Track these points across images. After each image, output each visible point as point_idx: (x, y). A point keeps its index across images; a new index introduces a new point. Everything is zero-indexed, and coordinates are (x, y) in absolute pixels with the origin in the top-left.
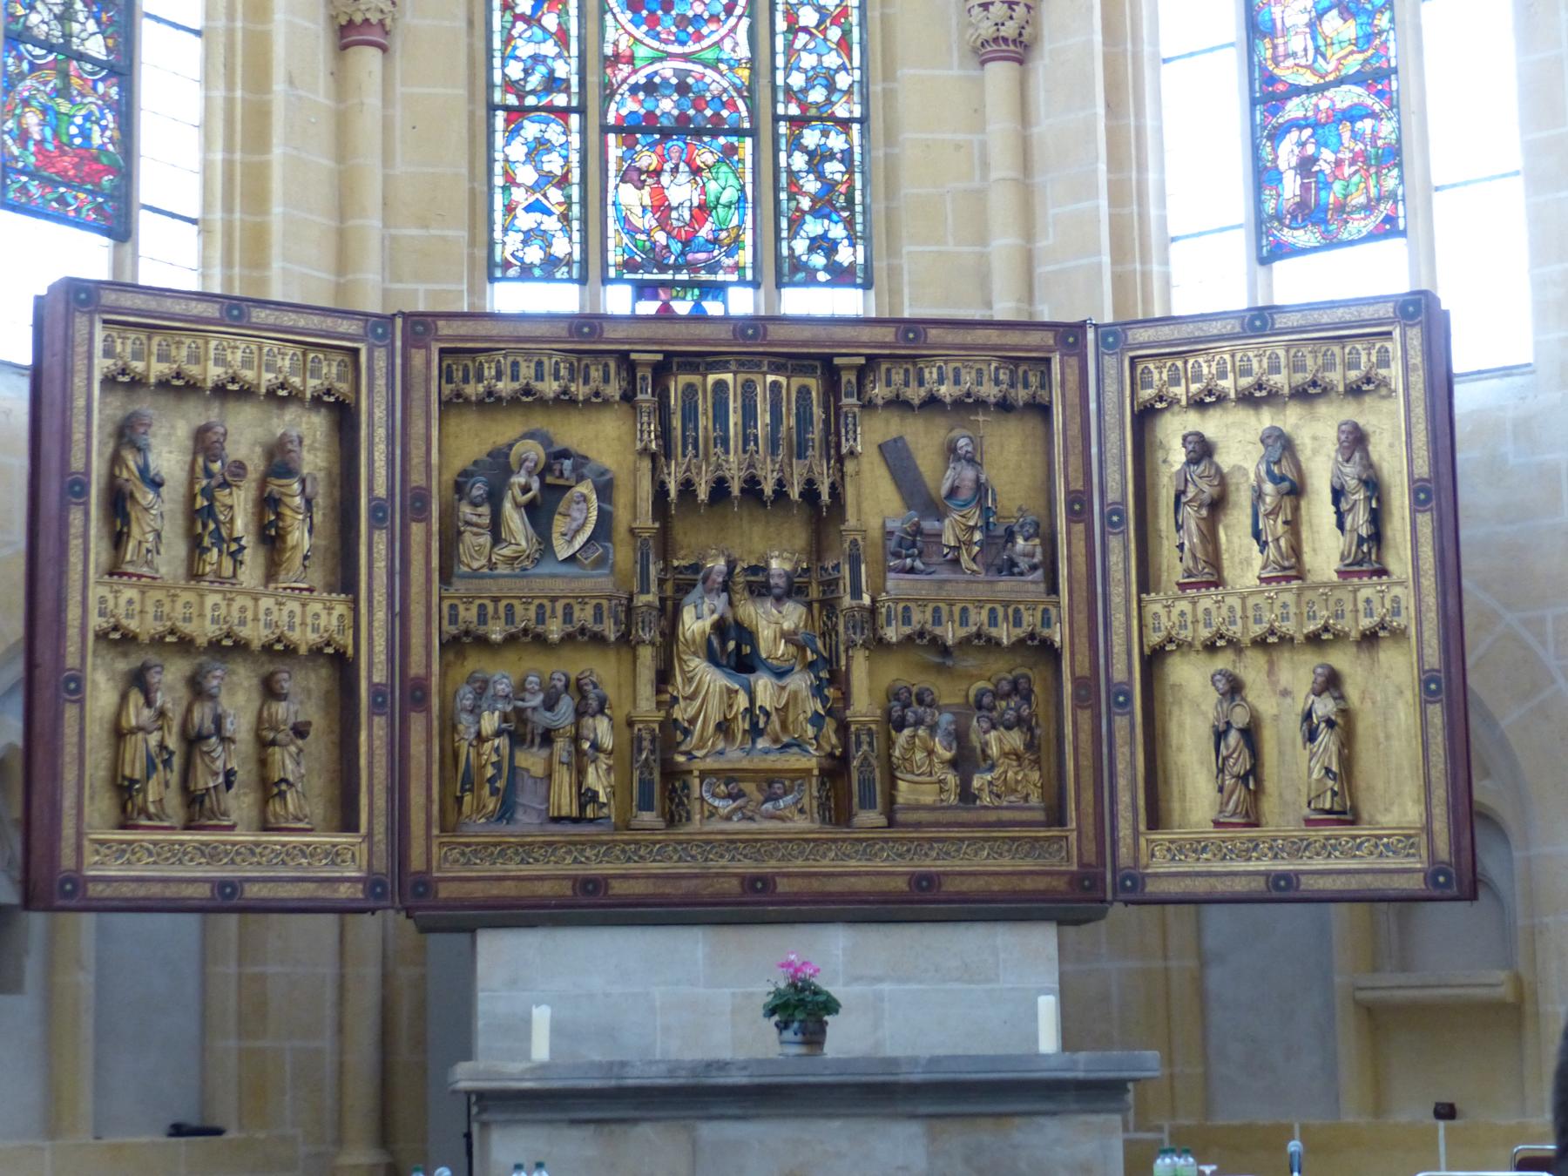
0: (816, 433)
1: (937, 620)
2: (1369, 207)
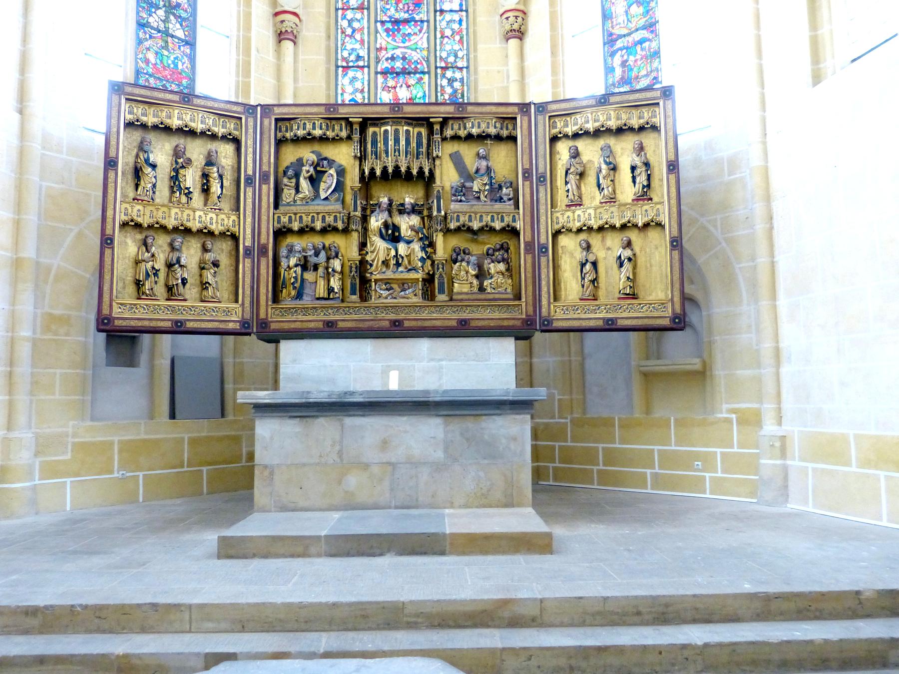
0: (424, 149)
1: (470, 220)
2: (647, 75)
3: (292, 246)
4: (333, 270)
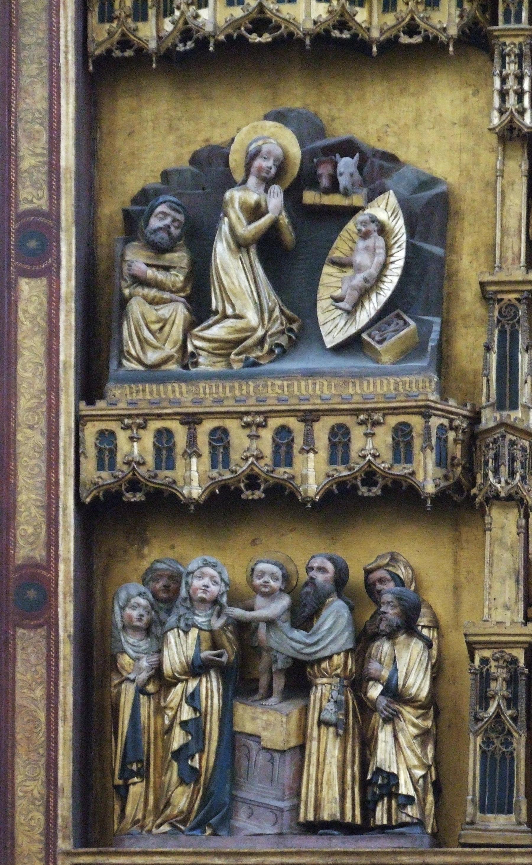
3: (176, 578)
4: (394, 692)
